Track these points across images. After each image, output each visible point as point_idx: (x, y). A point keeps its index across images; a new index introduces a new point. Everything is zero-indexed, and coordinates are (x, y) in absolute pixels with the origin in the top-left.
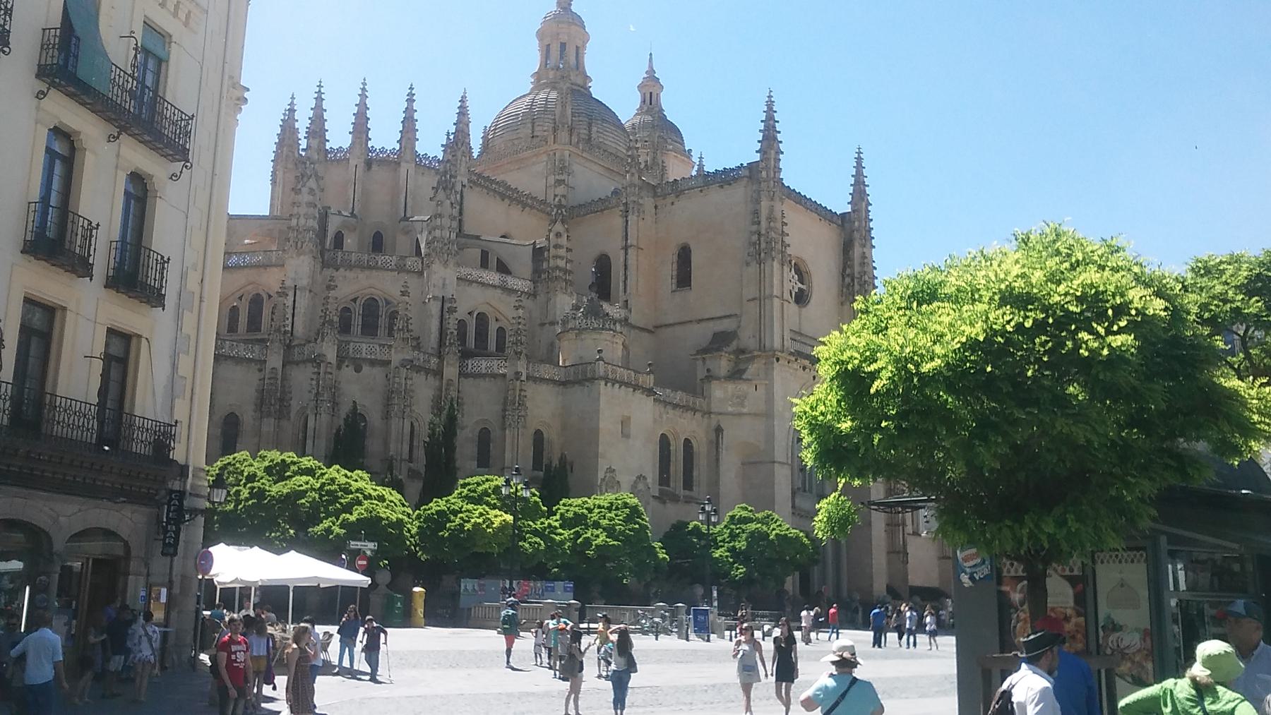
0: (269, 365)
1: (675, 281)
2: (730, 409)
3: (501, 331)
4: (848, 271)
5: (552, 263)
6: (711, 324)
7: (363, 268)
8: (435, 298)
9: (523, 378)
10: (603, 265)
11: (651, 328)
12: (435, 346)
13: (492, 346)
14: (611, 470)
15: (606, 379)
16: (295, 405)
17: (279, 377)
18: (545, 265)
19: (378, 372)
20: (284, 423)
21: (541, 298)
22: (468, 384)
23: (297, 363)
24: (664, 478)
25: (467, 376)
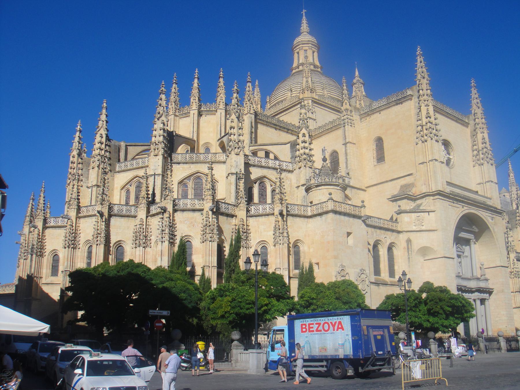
0: (139, 217)
1: (375, 160)
2: (414, 228)
3: (273, 191)
4: (475, 147)
5: (302, 151)
6: (399, 181)
7: (193, 163)
8: (232, 174)
9: (285, 213)
10: (335, 155)
11: (363, 188)
12: (234, 201)
13: (269, 200)
14: (342, 266)
15: (335, 212)
16: (153, 239)
17: (144, 223)
18: (298, 153)
19: (197, 214)
20: (148, 249)
21: (297, 171)
22: (252, 221)
23: (154, 215)
24: (377, 272)
25: (251, 216)
